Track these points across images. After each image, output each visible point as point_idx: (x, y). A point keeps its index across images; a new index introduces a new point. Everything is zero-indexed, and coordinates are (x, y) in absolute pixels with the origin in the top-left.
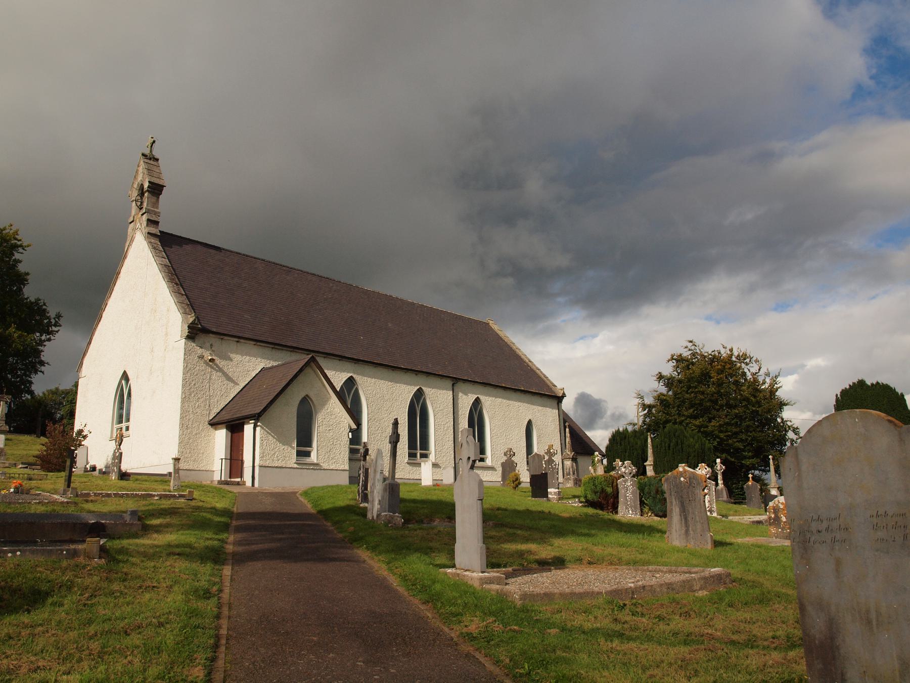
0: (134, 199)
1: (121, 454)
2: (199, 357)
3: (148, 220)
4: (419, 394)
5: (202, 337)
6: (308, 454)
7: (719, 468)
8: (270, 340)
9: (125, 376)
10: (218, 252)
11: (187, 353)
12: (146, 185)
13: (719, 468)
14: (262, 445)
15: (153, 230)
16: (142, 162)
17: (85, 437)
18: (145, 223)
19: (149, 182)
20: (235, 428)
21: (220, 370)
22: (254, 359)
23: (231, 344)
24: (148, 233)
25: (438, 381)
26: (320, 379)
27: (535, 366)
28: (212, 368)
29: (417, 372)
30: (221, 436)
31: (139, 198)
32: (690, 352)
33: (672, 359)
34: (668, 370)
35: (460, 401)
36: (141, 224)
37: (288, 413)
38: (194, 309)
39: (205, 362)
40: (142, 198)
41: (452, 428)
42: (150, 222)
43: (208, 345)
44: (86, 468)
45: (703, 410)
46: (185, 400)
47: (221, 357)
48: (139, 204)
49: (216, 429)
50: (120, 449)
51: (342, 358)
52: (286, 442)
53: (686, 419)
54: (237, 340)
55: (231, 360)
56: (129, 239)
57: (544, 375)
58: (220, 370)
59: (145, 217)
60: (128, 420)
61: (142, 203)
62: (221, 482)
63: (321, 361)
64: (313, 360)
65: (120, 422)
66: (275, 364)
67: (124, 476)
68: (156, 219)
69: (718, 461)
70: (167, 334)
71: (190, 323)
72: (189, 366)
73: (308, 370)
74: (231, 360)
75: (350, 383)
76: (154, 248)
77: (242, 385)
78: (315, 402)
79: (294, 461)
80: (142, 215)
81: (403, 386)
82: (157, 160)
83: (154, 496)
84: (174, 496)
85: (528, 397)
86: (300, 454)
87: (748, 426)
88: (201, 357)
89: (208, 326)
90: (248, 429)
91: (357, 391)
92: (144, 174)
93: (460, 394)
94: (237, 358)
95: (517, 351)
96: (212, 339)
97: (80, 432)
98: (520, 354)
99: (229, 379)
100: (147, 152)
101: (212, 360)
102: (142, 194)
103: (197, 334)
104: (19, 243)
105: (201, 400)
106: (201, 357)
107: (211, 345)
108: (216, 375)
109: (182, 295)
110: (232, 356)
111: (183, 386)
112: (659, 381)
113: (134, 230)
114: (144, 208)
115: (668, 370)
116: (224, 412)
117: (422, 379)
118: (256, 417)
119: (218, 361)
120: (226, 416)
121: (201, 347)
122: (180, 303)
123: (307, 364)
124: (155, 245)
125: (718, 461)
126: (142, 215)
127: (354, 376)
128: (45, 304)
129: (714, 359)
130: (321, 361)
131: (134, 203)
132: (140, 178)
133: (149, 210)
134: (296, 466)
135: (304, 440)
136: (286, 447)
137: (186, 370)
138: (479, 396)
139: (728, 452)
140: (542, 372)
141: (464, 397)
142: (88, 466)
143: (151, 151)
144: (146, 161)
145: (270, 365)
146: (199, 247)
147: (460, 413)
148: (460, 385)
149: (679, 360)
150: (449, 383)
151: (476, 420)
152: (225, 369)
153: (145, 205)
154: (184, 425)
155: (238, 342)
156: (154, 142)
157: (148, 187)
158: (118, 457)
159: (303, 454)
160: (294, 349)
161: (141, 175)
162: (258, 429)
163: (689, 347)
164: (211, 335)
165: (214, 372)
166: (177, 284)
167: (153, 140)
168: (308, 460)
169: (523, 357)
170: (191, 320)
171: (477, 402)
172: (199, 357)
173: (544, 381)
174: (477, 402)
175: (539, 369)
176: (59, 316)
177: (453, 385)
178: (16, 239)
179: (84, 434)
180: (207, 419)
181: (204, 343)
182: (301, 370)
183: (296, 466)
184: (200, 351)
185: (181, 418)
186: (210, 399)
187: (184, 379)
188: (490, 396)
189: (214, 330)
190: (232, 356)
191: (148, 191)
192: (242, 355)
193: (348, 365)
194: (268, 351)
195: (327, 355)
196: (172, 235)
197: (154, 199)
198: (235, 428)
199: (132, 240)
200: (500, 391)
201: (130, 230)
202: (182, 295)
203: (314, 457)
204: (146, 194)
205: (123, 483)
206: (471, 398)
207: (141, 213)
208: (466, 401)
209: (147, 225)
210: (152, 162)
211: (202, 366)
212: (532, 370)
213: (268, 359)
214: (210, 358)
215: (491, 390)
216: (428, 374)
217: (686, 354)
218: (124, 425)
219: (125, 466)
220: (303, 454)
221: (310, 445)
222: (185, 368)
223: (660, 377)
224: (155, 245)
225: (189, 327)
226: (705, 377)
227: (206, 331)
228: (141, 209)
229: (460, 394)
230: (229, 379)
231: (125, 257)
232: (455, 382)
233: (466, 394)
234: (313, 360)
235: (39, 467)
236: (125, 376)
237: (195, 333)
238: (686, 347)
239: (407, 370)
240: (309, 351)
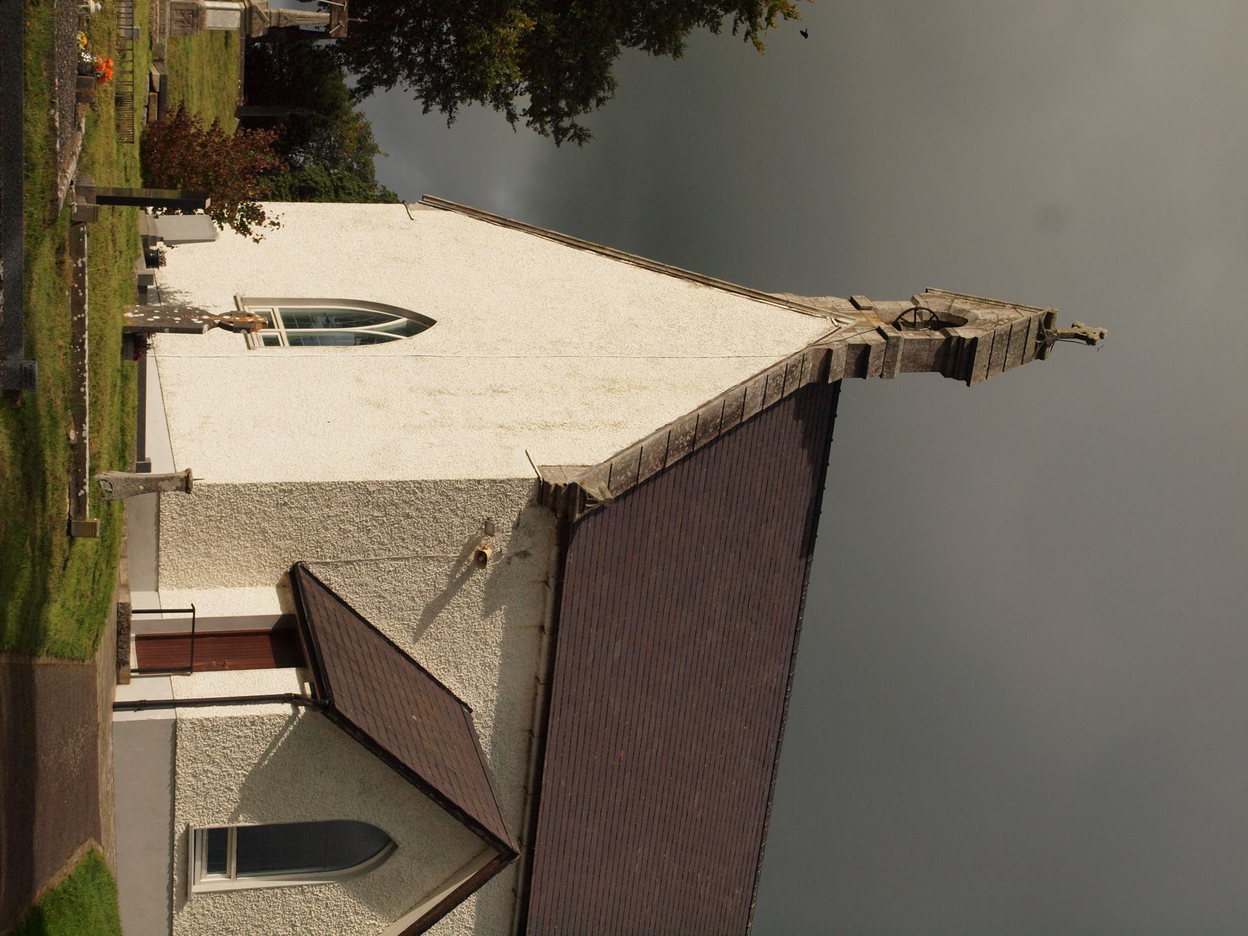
0: (922, 304)
1: (198, 330)
2: (487, 522)
3: (866, 348)
5: (546, 527)
6: (216, 864)
8: (554, 722)
9: (418, 324)
11: (498, 488)
12: (965, 333)
14: (239, 722)
16: (1027, 315)
17: (243, 229)
18: (857, 340)
19: (975, 340)
21: (455, 585)
22: (494, 679)
23: (535, 611)
24: (829, 352)
26: (446, 883)
28: (460, 562)
31: (926, 317)
36: (853, 329)
38: (625, 495)
39: (474, 542)
40: (926, 324)
42: (861, 358)
43: (526, 544)
44: (155, 240)
46: (362, 492)
47: (491, 584)
48: (910, 318)
49: (280, 587)
50: (211, 327)
52: (250, 794)
54: (547, 625)
55: (487, 614)
56: (807, 301)
59: (873, 338)
60: (295, 342)
61: (912, 326)
62: (124, 611)
63: (504, 880)
64: (506, 855)
65: (289, 321)
66: (485, 743)
68: (871, 369)
70: (546, 427)
71: (585, 487)
72: (463, 497)
73: (474, 843)
74: (487, 614)
76: (788, 372)
77: (415, 652)
78: (376, 874)
79: (196, 824)
80: (879, 331)
82: (1041, 355)
83: (79, 428)
84: (79, 484)
86: (216, 838)
88: (488, 528)
89: (581, 540)
90: (286, 680)
92: (997, 323)
94: (495, 629)
96: (543, 555)
99: (431, 613)
100: (1059, 326)
101: (481, 559)
102: (940, 322)
103: (554, 510)
104: (761, 21)
105: (364, 538)
107: (525, 554)
108: (439, 573)
109: (664, 460)
110: (499, 617)
111: (401, 485)
113: (835, 314)
114: (899, 334)
116: (330, 604)
119: (481, 576)
120: (319, 616)
121: (516, 526)
122: (639, 454)
123: (491, 839)
124: (797, 373)
126: (879, 331)
128: (600, 101)
130: (504, 880)
132: (982, 313)
133: (896, 346)
134: (180, 829)
136: (235, 795)
137: (447, 491)
142: (160, 245)
143: (1063, 336)
144: (1034, 326)
145: (478, 728)
152: (458, 599)
155: (542, 628)
156: (1091, 342)
157: (959, 338)
161: (993, 317)
162: (287, 709)
166: (693, 442)
167: (1096, 337)
168: (198, 865)
170: (593, 491)
172: (487, 522)
176: (581, 136)
178: (771, 12)
179: (253, 227)
180: (308, 559)
181: (530, 534)
182: (471, 823)
183: (180, 829)
184: (506, 522)
185: (308, 487)
186: (367, 562)
187: (420, 485)
189: (571, 558)
190: (499, 617)
191: (949, 338)
192: (502, 645)
195: (523, 899)
196: (832, 415)
197: (926, 357)
201: (831, 301)
202: (664, 460)
203: (206, 882)
204: (938, 335)
205: (114, 343)
207: (883, 326)
209: (851, 347)
210: (1032, 341)
211: (463, 532)
213: (498, 721)
214: (488, 552)
218: (281, 331)
219: (164, 345)
221: (245, 868)
222: (454, 486)
224: (797, 373)
225: (573, 486)
227: (565, 535)
228: (896, 325)
230: (431, 613)
231: (754, 296)
234: (506, 855)
235: (154, 117)
236: (418, 324)
240: (530, 843)
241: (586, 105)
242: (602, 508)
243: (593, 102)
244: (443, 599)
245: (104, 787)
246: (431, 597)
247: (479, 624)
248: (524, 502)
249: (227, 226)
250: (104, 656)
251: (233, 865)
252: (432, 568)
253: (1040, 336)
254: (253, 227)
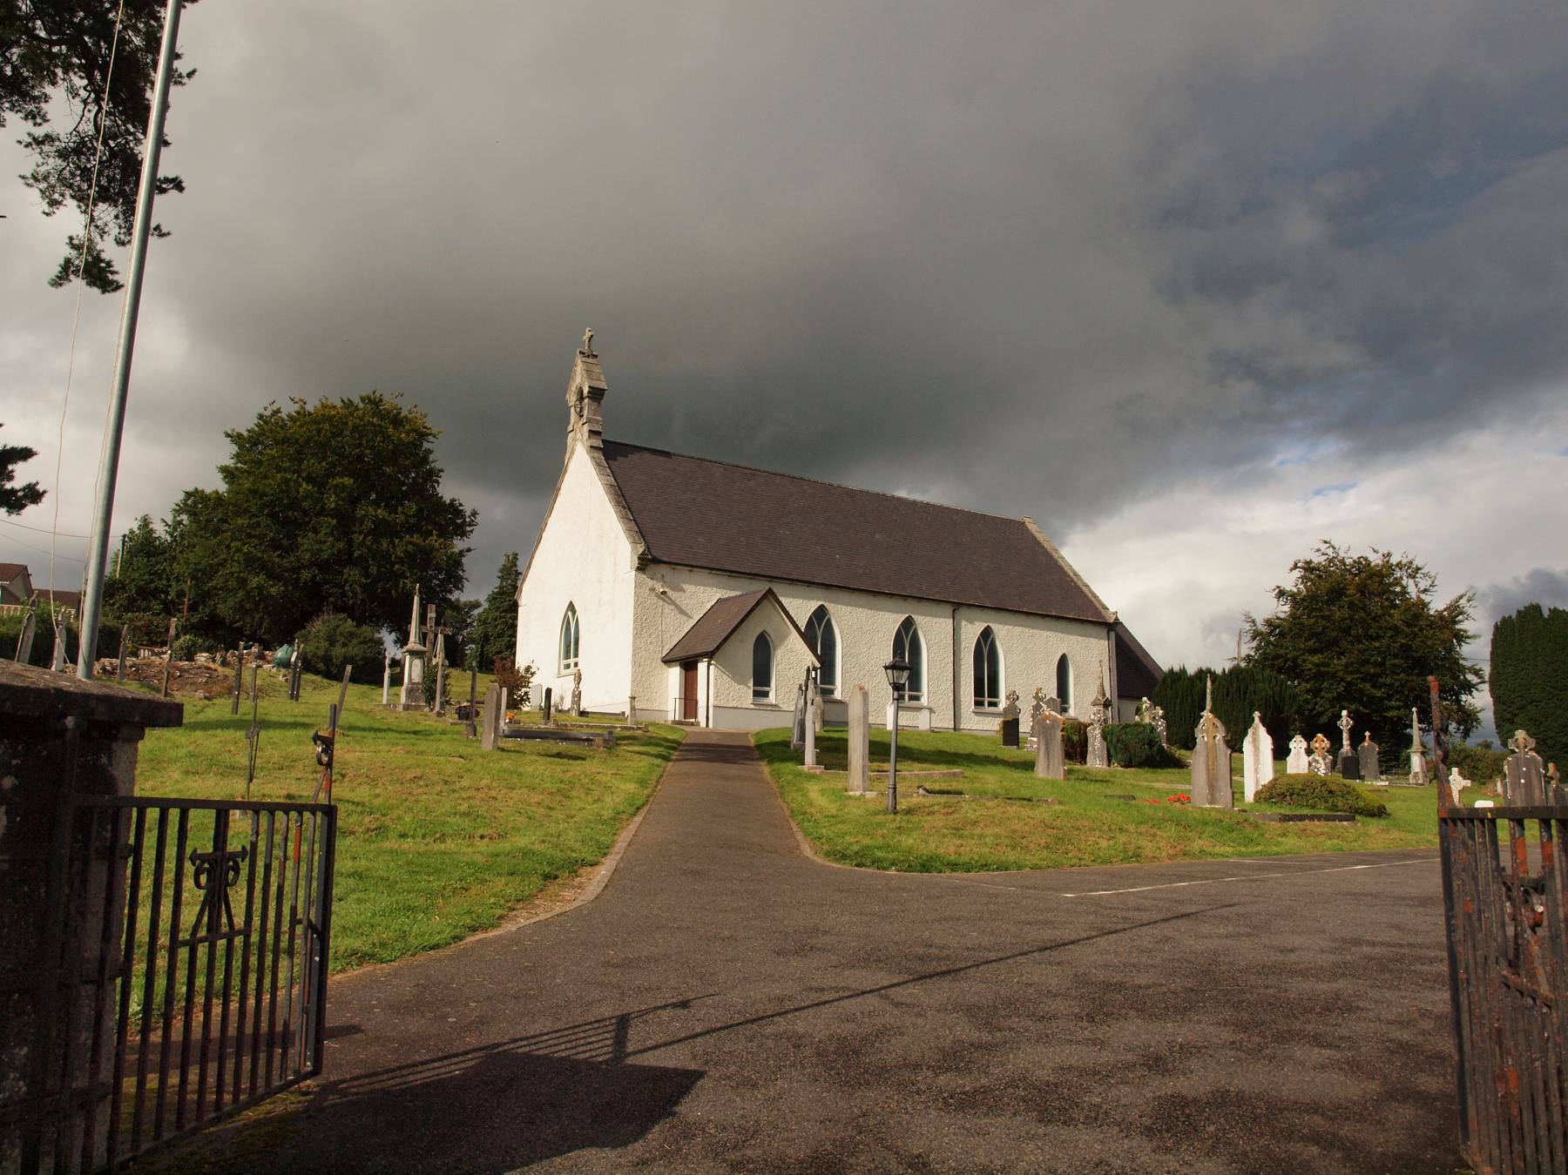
3: (590, 431)
4: (908, 624)
5: (653, 568)
6: (766, 694)
7: (1344, 722)
8: (727, 568)
9: (571, 607)
10: (668, 460)
11: (638, 585)
12: (586, 390)
13: (1344, 722)
14: (716, 684)
15: (598, 443)
16: (579, 362)
17: (533, 674)
18: (586, 435)
20: (689, 666)
21: (673, 603)
23: (683, 573)
25: (934, 607)
26: (779, 613)
27: (1082, 580)
28: (664, 601)
29: (906, 597)
30: (675, 674)
32: (1325, 557)
33: (1295, 567)
34: (1291, 581)
35: (963, 631)
37: (744, 651)
38: (643, 536)
39: (657, 595)
41: (951, 665)
42: (592, 433)
43: (660, 575)
45: (1326, 644)
46: (637, 636)
47: (673, 589)
51: (810, 584)
52: (741, 681)
53: (1303, 654)
55: (684, 591)
56: (569, 451)
57: (1093, 594)
58: (673, 603)
60: (576, 656)
61: (581, 409)
62: (674, 722)
64: (770, 591)
65: (567, 657)
67: (583, 714)
68: (599, 430)
69: (1344, 713)
72: (640, 600)
73: (765, 602)
74: (684, 591)
75: (821, 613)
78: (773, 638)
79: (751, 701)
81: (887, 615)
82: (596, 356)
85: (1063, 624)
86: (757, 694)
87: (1395, 665)
88: (652, 590)
89: (658, 555)
90: (702, 666)
91: (829, 621)
93: (964, 623)
94: (689, 588)
95: (1060, 561)
96: (663, 569)
97: (528, 669)
98: (1063, 565)
99: (682, 612)
101: (664, 593)
102: (581, 398)
104: (429, 431)
105: (653, 636)
106: (652, 590)
108: (668, 608)
110: (685, 586)
111: (635, 621)
112: (1279, 598)
113: (575, 440)
115: (1291, 581)
116: (677, 649)
117: (912, 605)
118: (710, 655)
119: (670, 593)
120: (680, 653)
122: (628, 530)
123: (764, 597)
125: (1344, 713)
127: (826, 604)
128: (461, 505)
129: (1362, 566)
131: (573, 409)
132: (578, 380)
134: (752, 706)
135: (762, 678)
136: (742, 686)
137: (638, 604)
138: (990, 625)
139: (1361, 703)
140: (1090, 590)
141: (969, 625)
146: (647, 455)
147: (963, 646)
148: (964, 611)
149: (1309, 568)
150: (949, 609)
151: (986, 653)
152: (678, 602)
153: (585, 412)
154: (636, 663)
157: (589, 392)
158: (577, 696)
159: (760, 694)
160: (753, 576)
162: (712, 667)
163: (1323, 550)
164: (662, 565)
165: (666, 606)
166: (624, 508)
167: (590, 334)
168: (765, 701)
169: (1066, 569)
170: (641, 550)
171: (987, 634)
173: (1092, 602)
174: (987, 634)
175: (1087, 586)
176: (474, 514)
177: (954, 611)
178: (425, 428)
179: (532, 670)
180: (660, 656)
181: (655, 574)
182: (757, 604)
183: (752, 706)
184: (650, 583)
185: (634, 655)
187: (635, 615)
188: (1006, 624)
189: (665, 559)
190: (685, 586)
192: (696, 585)
193: (819, 592)
194: (724, 580)
195: (793, 581)
197: (594, 406)
198: (689, 666)
199: (572, 453)
200: (1021, 618)
201: (569, 440)
203: (772, 698)
204: (586, 400)
205: (583, 719)
206: (979, 627)
208: (971, 632)
209: (589, 437)
210: (590, 360)
212: (1076, 586)
213: (724, 588)
215: (1007, 616)
216: (920, 599)
217: (1318, 559)
218: (572, 661)
220: (760, 694)
221: (768, 684)
223: (1281, 593)
226: (1337, 593)
227: (656, 561)
228: (582, 416)
229: (964, 623)
230: (682, 612)
231: (566, 471)
232: (957, 606)
233: (972, 623)
234: (770, 591)
236: (571, 607)
237: (645, 563)
238: (1319, 550)
239: (892, 595)
241: (462, 511)
242: (648, 547)
243: (461, 508)
244: (677, 606)
245: (734, 731)
246: (677, 612)
247: (688, 594)
248: (644, 576)
249: (531, 680)
250: (688, 729)
251: (766, 689)
252: (666, 611)
253: (588, 356)
254: (532, 670)
